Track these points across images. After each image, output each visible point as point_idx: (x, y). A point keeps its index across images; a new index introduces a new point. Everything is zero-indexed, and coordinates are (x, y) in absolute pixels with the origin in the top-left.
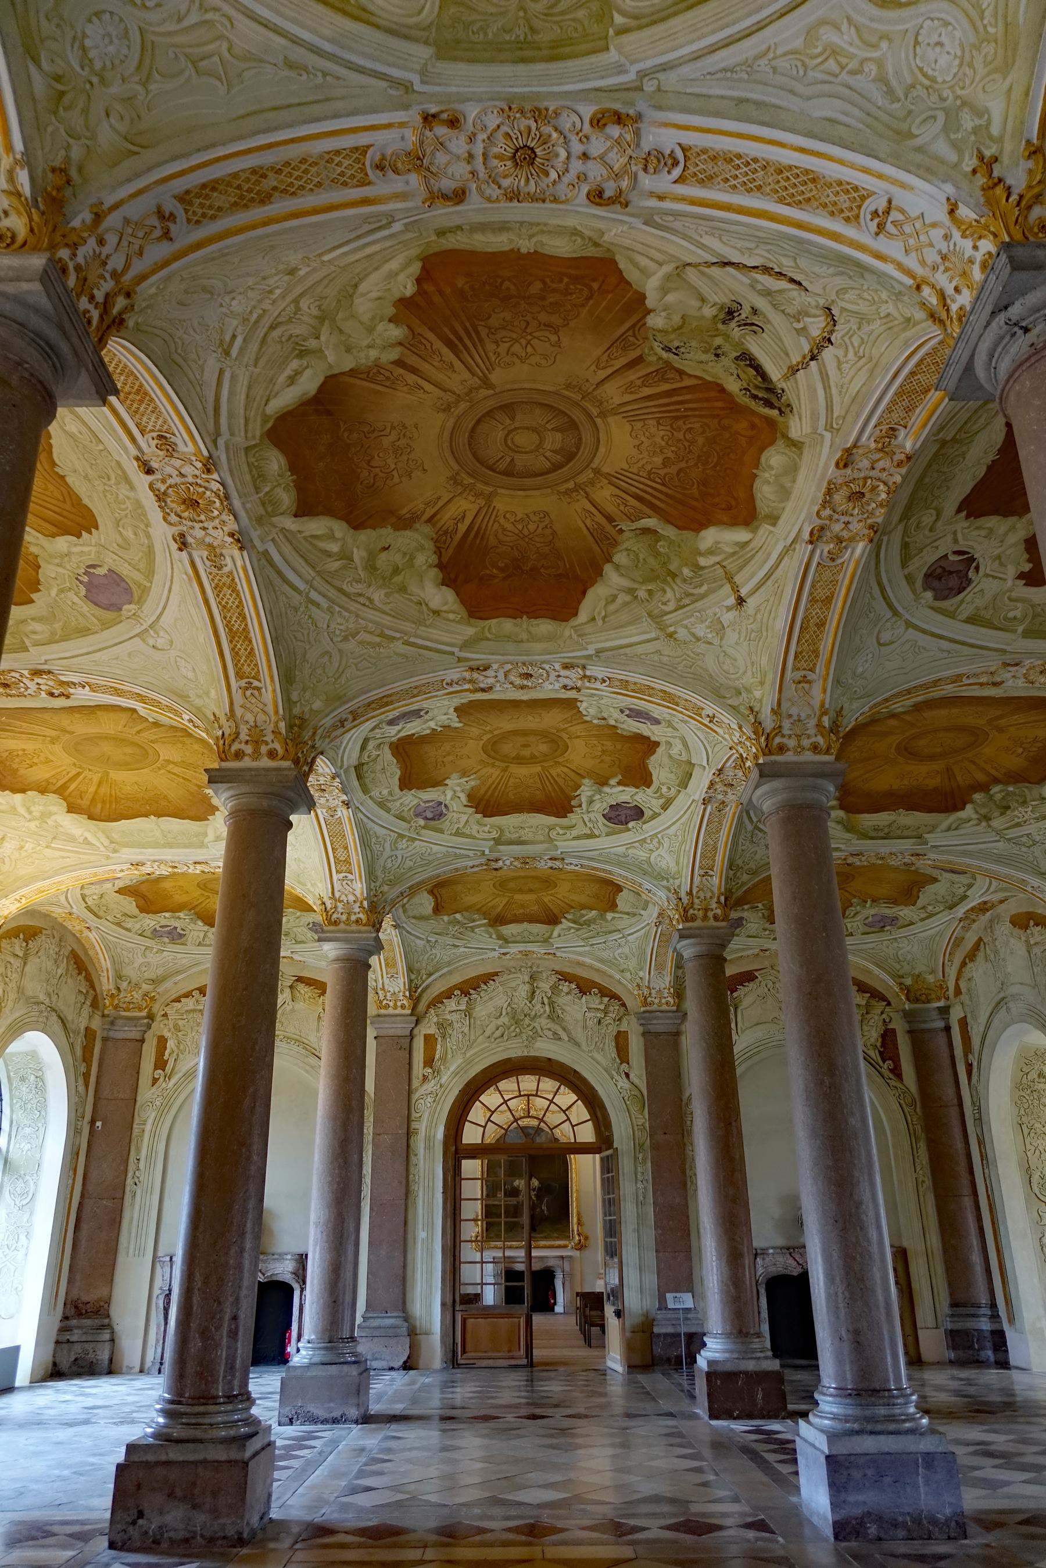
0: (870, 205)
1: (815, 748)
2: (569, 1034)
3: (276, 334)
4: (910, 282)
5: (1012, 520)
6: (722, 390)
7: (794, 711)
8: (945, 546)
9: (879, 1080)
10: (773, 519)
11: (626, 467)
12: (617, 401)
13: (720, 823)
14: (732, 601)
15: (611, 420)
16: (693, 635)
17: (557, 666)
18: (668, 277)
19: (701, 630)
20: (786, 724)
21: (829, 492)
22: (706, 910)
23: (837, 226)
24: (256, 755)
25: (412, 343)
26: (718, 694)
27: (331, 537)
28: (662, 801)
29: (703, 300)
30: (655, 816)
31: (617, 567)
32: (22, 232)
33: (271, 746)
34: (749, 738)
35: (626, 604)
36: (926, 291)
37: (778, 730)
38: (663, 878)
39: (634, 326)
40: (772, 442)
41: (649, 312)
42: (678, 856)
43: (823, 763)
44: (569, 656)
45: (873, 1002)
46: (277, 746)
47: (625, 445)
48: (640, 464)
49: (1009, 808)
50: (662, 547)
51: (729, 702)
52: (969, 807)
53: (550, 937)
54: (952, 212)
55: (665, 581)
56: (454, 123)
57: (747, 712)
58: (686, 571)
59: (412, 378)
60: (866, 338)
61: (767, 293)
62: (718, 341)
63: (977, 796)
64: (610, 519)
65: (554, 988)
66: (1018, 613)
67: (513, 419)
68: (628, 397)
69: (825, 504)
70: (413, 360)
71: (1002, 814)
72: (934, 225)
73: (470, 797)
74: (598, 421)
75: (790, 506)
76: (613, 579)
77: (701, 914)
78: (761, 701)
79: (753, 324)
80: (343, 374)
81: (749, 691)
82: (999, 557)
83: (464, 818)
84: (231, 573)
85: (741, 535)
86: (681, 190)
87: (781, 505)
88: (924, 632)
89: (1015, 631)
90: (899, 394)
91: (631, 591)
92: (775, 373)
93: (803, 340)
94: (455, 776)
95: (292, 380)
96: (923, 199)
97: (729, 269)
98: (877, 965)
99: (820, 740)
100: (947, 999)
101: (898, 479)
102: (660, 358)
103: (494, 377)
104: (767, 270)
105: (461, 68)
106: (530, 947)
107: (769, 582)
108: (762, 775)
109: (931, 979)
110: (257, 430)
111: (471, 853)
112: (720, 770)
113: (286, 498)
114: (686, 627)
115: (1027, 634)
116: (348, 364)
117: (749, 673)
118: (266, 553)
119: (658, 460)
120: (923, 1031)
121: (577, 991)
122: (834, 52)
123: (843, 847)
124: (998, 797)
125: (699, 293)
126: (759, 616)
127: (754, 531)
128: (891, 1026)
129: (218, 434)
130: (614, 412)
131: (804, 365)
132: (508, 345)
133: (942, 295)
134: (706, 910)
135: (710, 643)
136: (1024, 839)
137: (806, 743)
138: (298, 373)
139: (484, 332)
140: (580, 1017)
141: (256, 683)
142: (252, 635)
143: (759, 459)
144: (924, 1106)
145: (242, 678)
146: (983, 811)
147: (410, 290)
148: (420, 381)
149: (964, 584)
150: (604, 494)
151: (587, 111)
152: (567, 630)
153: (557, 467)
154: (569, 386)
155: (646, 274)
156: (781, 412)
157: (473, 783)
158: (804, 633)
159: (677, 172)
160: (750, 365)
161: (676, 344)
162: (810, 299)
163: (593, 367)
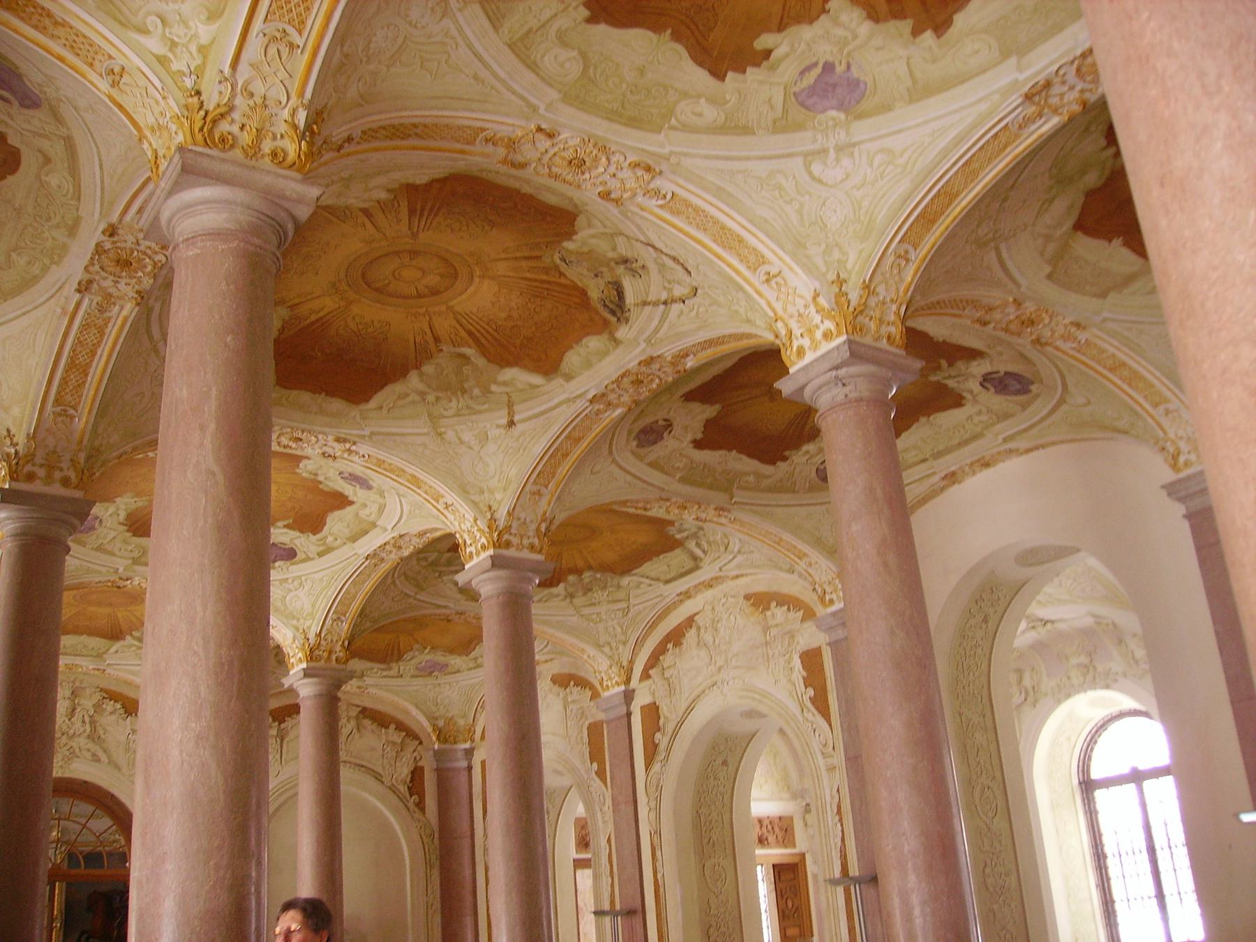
0: (766, 268)
1: (532, 547)
2: (109, 756)
4: (772, 314)
5: (705, 406)
6: (584, 292)
7: (523, 516)
8: (660, 415)
9: (404, 812)
10: (569, 378)
11: (475, 310)
13: (369, 576)
14: (504, 421)
15: (486, 283)
16: (460, 439)
17: (330, 438)
19: (466, 437)
20: (515, 525)
21: (623, 376)
22: (330, 652)
23: (742, 268)
24: (49, 479)
26: (463, 490)
28: (321, 548)
29: (614, 249)
30: (308, 559)
31: (421, 375)
32: (292, 155)
33: (66, 473)
34: (479, 530)
35: (413, 402)
36: (780, 324)
37: (508, 528)
38: (294, 617)
40: (599, 333)
42: (316, 600)
43: (538, 562)
44: (344, 432)
45: (408, 741)
46: (72, 475)
47: (482, 298)
49: (590, 590)
50: (467, 370)
51: (472, 497)
52: (562, 586)
53: (105, 653)
54: (814, 298)
55: (454, 393)
56: (551, 136)
57: (486, 509)
58: (476, 391)
62: (604, 269)
63: (571, 578)
64: (437, 340)
65: (98, 707)
66: (681, 465)
68: (511, 274)
69: (618, 381)
71: (585, 594)
72: (800, 296)
73: (129, 516)
74: (477, 280)
76: (414, 380)
77: (326, 655)
78: (500, 503)
81: (491, 492)
82: (686, 427)
83: (113, 534)
84: (109, 318)
85: (536, 379)
86: (657, 211)
88: (620, 467)
89: (674, 477)
91: (423, 394)
92: (630, 299)
94: (129, 494)
96: (802, 283)
98: (417, 707)
99: (536, 541)
100: (473, 741)
101: (670, 379)
104: (674, 259)
105: (572, 111)
106: (78, 661)
108: (493, 565)
109: (461, 722)
111: (104, 570)
112: (401, 536)
114: (456, 431)
115: (683, 480)
117: (497, 478)
118: (151, 310)
119: (503, 315)
120: (448, 769)
121: (122, 711)
122: (780, 188)
123: (452, 605)
124: (587, 580)
127: (549, 381)
128: (420, 764)
130: (492, 278)
131: (656, 304)
133: (790, 333)
134: (330, 652)
135: (470, 448)
136: (594, 616)
137: (526, 542)
140: (123, 738)
141: (72, 411)
142: (92, 370)
144: (441, 838)
145: (59, 405)
146: (571, 590)
149: (660, 437)
150: (444, 325)
151: (632, 158)
152: (355, 411)
153: (420, 296)
155: (590, 225)
157: (140, 504)
158: (555, 455)
159: (661, 202)
162: (688, 280)
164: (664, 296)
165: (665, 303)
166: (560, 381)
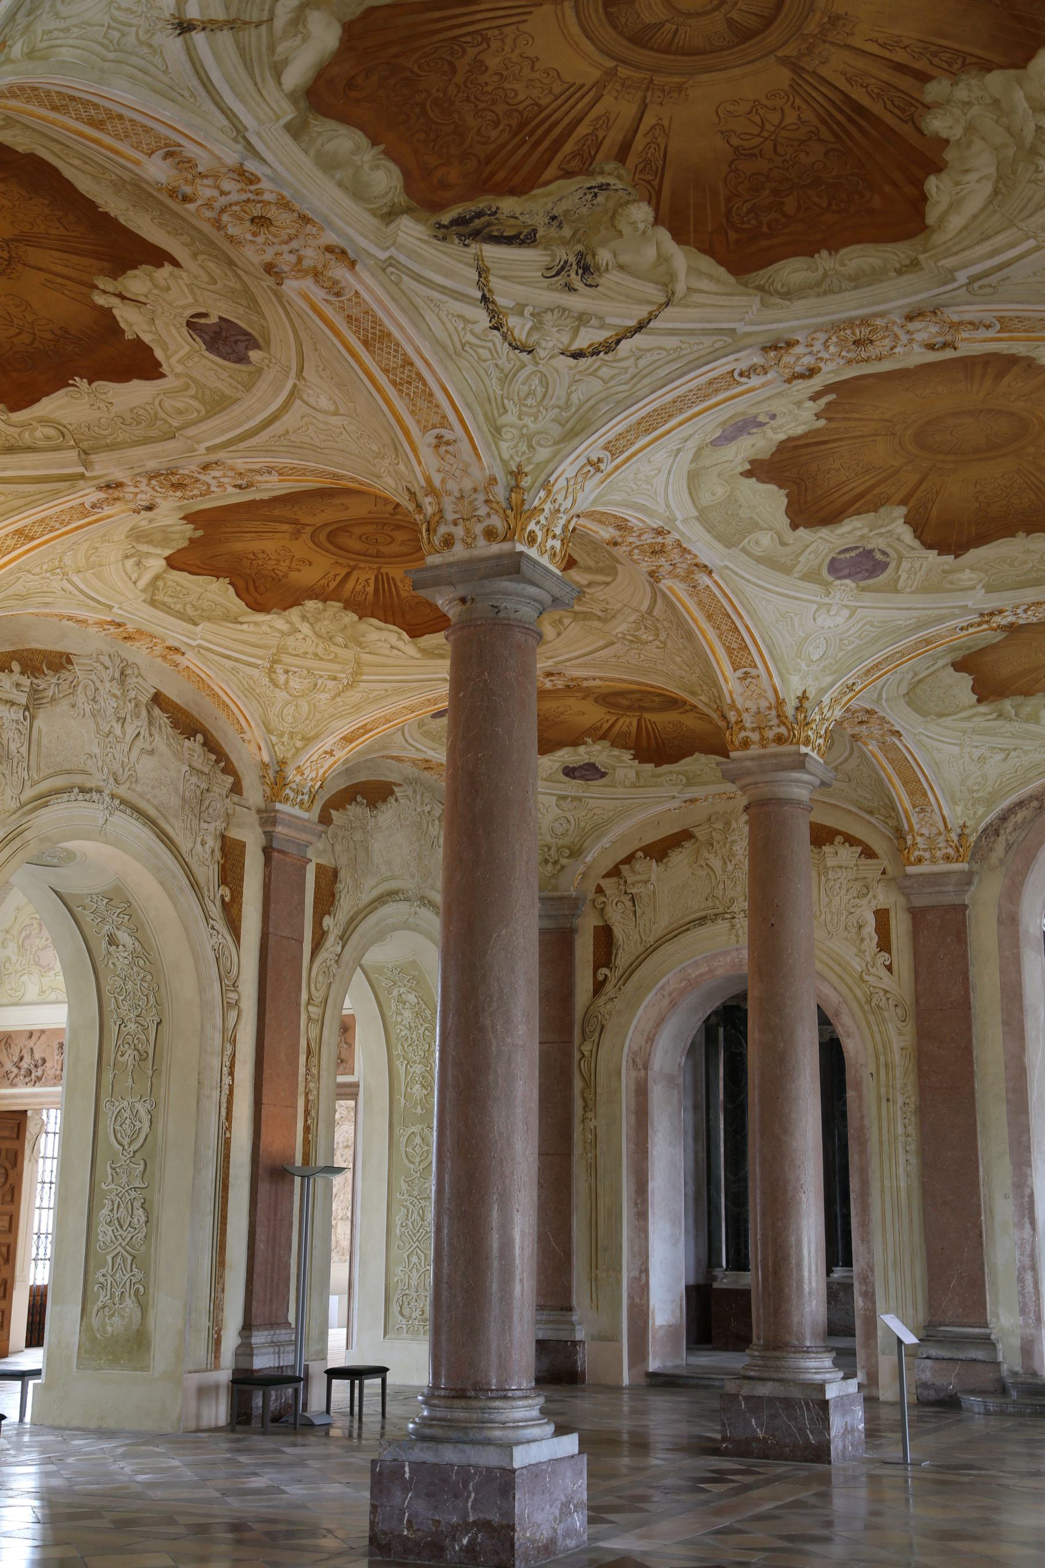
10: (296, 130)
11: (523, 27)
12: (608, 100)
14: (193, 12)
15: (596, 74)
18: (672, 276)
25: (915, 109)
29: (621, 267)
39: (659, 194)
40: (408, 189)
41: (657, 221)
48: (509, 42)
59: (900, 56)
60: (485, 365)
61: (582, 319)
62: (567, 232)
67: (730, 22)
70: (906, 83)
74: (610, 64)
75: (307, 163)
79: (558, 274)
80: (1001, 67)
85: (296, 75)
87: (312, 152)
92: (491, 252)
93: (511, 304)
97: (633, 323)
102: (602, 173)
103: (785, 75)
104: (608, 347)
107: (195, 83)
116: (995, 79)
119: (493, 62)
125: (630, 273)
126: (145, 50)
127: (293, 97)
130: (600, 86)
132: (787, 121)
139: (824, 133)
143: (396, 161)
147: (932, 184)
148: (887, 54)
154: (680, 88)
156: (441, 226)
160: (516, 237)
161: (600, 199)
163: (666, 123)
166: (289, 113)
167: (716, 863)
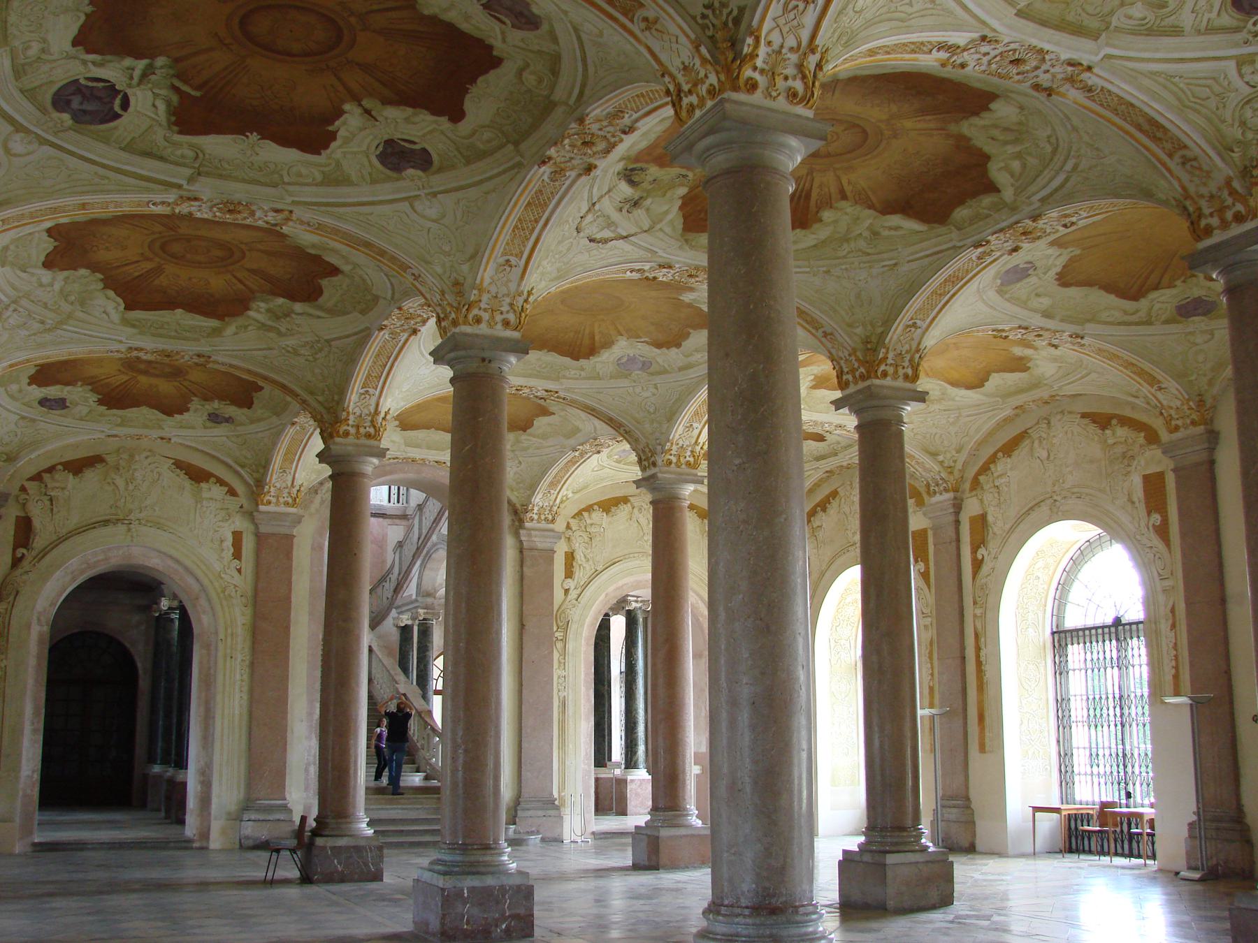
3: (869, 251)
27: (1007, 168)
29: (648, 210)
41: (683, 197)
90: (546, 205)
95: (897, 228)
110: (942, 229)
113: (987, 200)
118: (1042, 200)
129: (954, 247)
138: (890, 228)
155: (671, 221)
164: (597, 207)
165: (594, 204)
167: (120, 482)
